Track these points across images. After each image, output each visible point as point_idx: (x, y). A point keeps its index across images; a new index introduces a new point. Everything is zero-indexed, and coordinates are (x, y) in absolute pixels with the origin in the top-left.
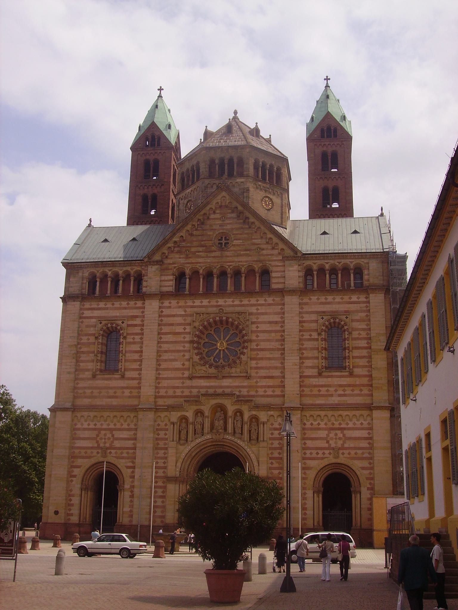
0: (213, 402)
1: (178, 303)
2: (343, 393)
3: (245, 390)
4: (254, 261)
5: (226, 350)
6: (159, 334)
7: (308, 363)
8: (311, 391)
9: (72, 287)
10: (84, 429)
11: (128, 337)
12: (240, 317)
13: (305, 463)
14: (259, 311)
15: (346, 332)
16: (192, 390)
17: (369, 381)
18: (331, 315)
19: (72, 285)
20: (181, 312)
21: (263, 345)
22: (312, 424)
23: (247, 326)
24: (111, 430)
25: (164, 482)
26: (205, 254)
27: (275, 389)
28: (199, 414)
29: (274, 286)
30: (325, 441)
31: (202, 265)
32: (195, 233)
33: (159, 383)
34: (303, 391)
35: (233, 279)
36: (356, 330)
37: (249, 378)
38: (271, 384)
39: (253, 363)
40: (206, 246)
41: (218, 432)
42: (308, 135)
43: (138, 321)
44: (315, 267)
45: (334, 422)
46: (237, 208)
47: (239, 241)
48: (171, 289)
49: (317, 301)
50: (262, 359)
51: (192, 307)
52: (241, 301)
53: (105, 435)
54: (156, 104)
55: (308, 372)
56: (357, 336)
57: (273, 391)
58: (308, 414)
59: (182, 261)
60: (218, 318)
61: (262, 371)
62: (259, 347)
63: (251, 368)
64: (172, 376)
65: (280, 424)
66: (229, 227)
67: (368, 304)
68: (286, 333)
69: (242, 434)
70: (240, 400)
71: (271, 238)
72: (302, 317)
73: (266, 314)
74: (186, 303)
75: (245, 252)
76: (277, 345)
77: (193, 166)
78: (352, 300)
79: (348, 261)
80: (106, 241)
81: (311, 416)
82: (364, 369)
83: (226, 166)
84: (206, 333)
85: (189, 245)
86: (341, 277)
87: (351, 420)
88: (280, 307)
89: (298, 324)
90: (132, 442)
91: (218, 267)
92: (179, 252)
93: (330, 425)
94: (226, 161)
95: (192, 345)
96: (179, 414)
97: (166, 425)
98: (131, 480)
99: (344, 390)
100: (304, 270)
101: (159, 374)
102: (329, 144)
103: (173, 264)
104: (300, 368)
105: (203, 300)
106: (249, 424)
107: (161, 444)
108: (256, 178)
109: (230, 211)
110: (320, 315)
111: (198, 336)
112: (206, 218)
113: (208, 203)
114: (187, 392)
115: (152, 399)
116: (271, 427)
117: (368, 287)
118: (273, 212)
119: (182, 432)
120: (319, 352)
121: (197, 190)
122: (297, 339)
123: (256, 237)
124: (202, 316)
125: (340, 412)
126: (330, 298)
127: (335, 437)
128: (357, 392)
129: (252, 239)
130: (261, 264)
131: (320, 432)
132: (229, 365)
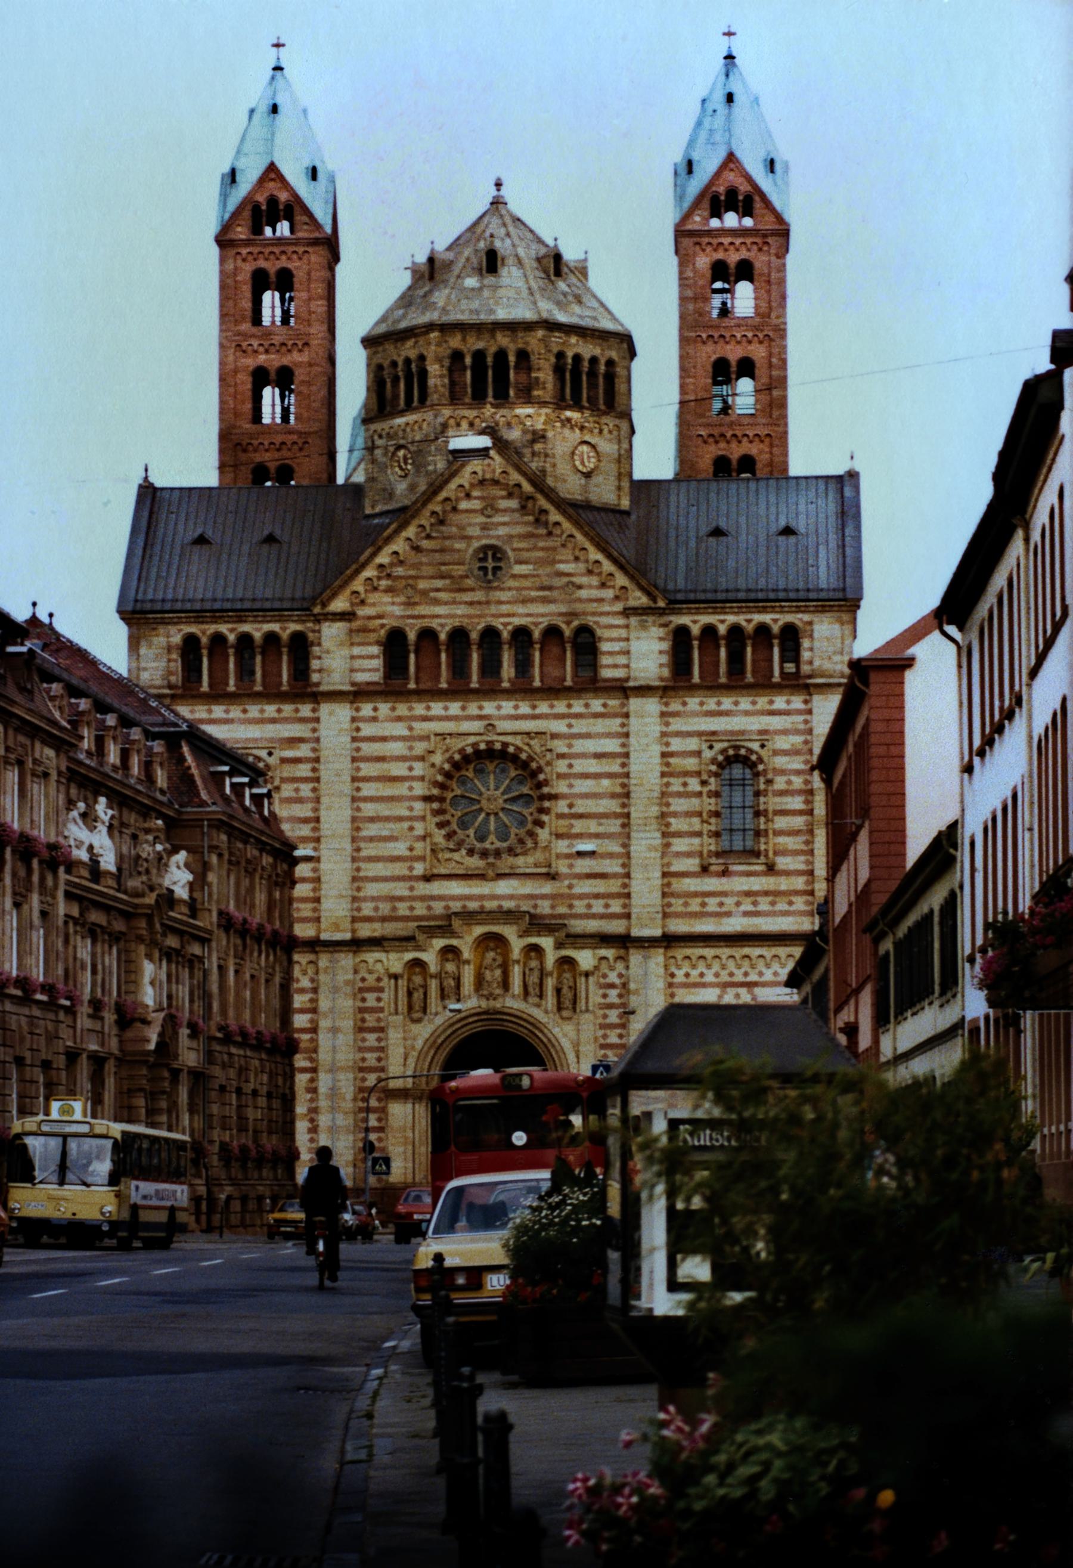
0: (479, 930)
1: (393, 709)
2: (750, 908)
4: (561, 614)
5: (501, 814)
6: (354, 779)
7: (680, 845)
8: (686, 904)
9: (145, 669)
11: (284, 786)
12: (532, 743)
14: (574, 730)
15: (762, 780)
16: (432, 904)
17: (807, 883)
19: (143, 665)
20: (400, 729)
21: (581, 807)
22: (687, 975)
23: (549, 764)
25: (379, 1100)
27: (611, 902)
28: (450, 956)
29: (606, 673)
31: (443, 621)
32: (425, 544)
33: (359, 889)
34: (669, 905)
35: (513, 652)
36: (783, 772)
37: (554, 878)
39: (562, 846)
40: (451, 577)
41: (491, 994)
42: (677, 220)
43: (304, 751)
44: (695, 630)
46: (519, 486)
47: (524, 567)
48: (377, 677)
49: (698, 708)
50: (579, 836)
52: (534, 707)
54: (271, 102)
55: (678, 866)
57: (607, 906)
58: (680, 953)
59: (397, 610)
62: (573, 811)
63: (558, 856)
64: (388, 873)
65: (620, 976)
66: (502, 531)
67: (808, 717)
68: (633, 781)
69: (541, 996)
70: (536, 924)
71: (597, 562)
72: (667, 744)
73: (588, 736)
74: (411, 709)
76: (613, 806)
77: (408, 361)
78: (775, 706)
79: (766, 618)
80: (201, 540)
81: (688, 957)
83: (490, 373)
84: (458, 775)
85: (412, 573)
86: (753, 653)
87: (768, 966)
88: (619, 721)
89: (657, 760)
90: (308, 1016)
91: (479, 627)
92: (389, 590)
93: (724, 977)
94: (490, 360)
95: (428, 806)
96: (409, 956)
97: (379, 980)
98: (309, 1096)
99: (755, 903)
100: (671, 637)
101: (358, 869)
102: (732, 244)
104: (662, 857)
106: (555, 975)
107: (371, 1020)
108: (560, 403)
109: (504, 493)
111: (442, 786)
112: (449, 508)
113: (453, 475)
114: (420, 910)
116: (602, 980)
117: (810, 677)
118: (597, 479)
119: (416, 995)
120: (703, 822)
121: (420, 428)
122: (656, 794)
123: (563, 558)
124: (448, 741)
125: (746, 951)
126: (727, 703)
128: (782, 906)
129: (554, 562)
130: (576, 623)
131: (702, 991)
132: (511, 851)
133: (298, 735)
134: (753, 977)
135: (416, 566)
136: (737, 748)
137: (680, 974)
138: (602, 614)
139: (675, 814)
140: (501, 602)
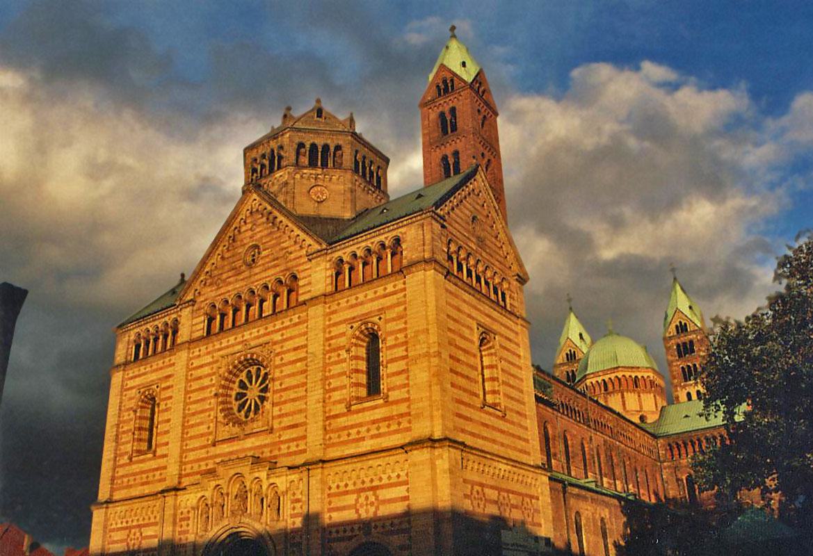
0: (232, 472)
3: (268, 450)
7: (336, 396)
8: (339, 437)
10: (119, 529)
11: (162, 403)
13: (331, 548)
18: (361, 320)
21: (289, 382)
24: (139, 526)
26: (235, 278)
27: (300, 442)
30: (354, 510)
36: (391, 333)
37: (271, 433)
38: (294, 436)
39: (276, 411)
40: (236, 268)
45: (365, 479)
50: (285, 402)
51: (220, 350)
53: (135, 535)
56: (394, 343)
57: (297, 446)
59: (213, 294)
60: (242, 358)
61: (285, 419)
62: (283, 386)
66: (259, 236)
69: (262, 513)
73: (291, 338)
75: (273, 263)
82: (403, 390)
85: (220, 272)
87: (384, 472)
92: (211, 284)
93: (359, 486)
97: (189, 512)
103: (206, 300)
105: (230, 338)
110: (349, 324)
115: (176, 481)
122: (321, 365)
126: (361, 297)
127: (365, 503)
129: (280, 243)
133: (170, 373)
134: (376, 483)
135: (223, 267)
136: (366, 323)
137: (334, 486)
138: (300, 265)
139: (333, 377)
140: (257, 274)
